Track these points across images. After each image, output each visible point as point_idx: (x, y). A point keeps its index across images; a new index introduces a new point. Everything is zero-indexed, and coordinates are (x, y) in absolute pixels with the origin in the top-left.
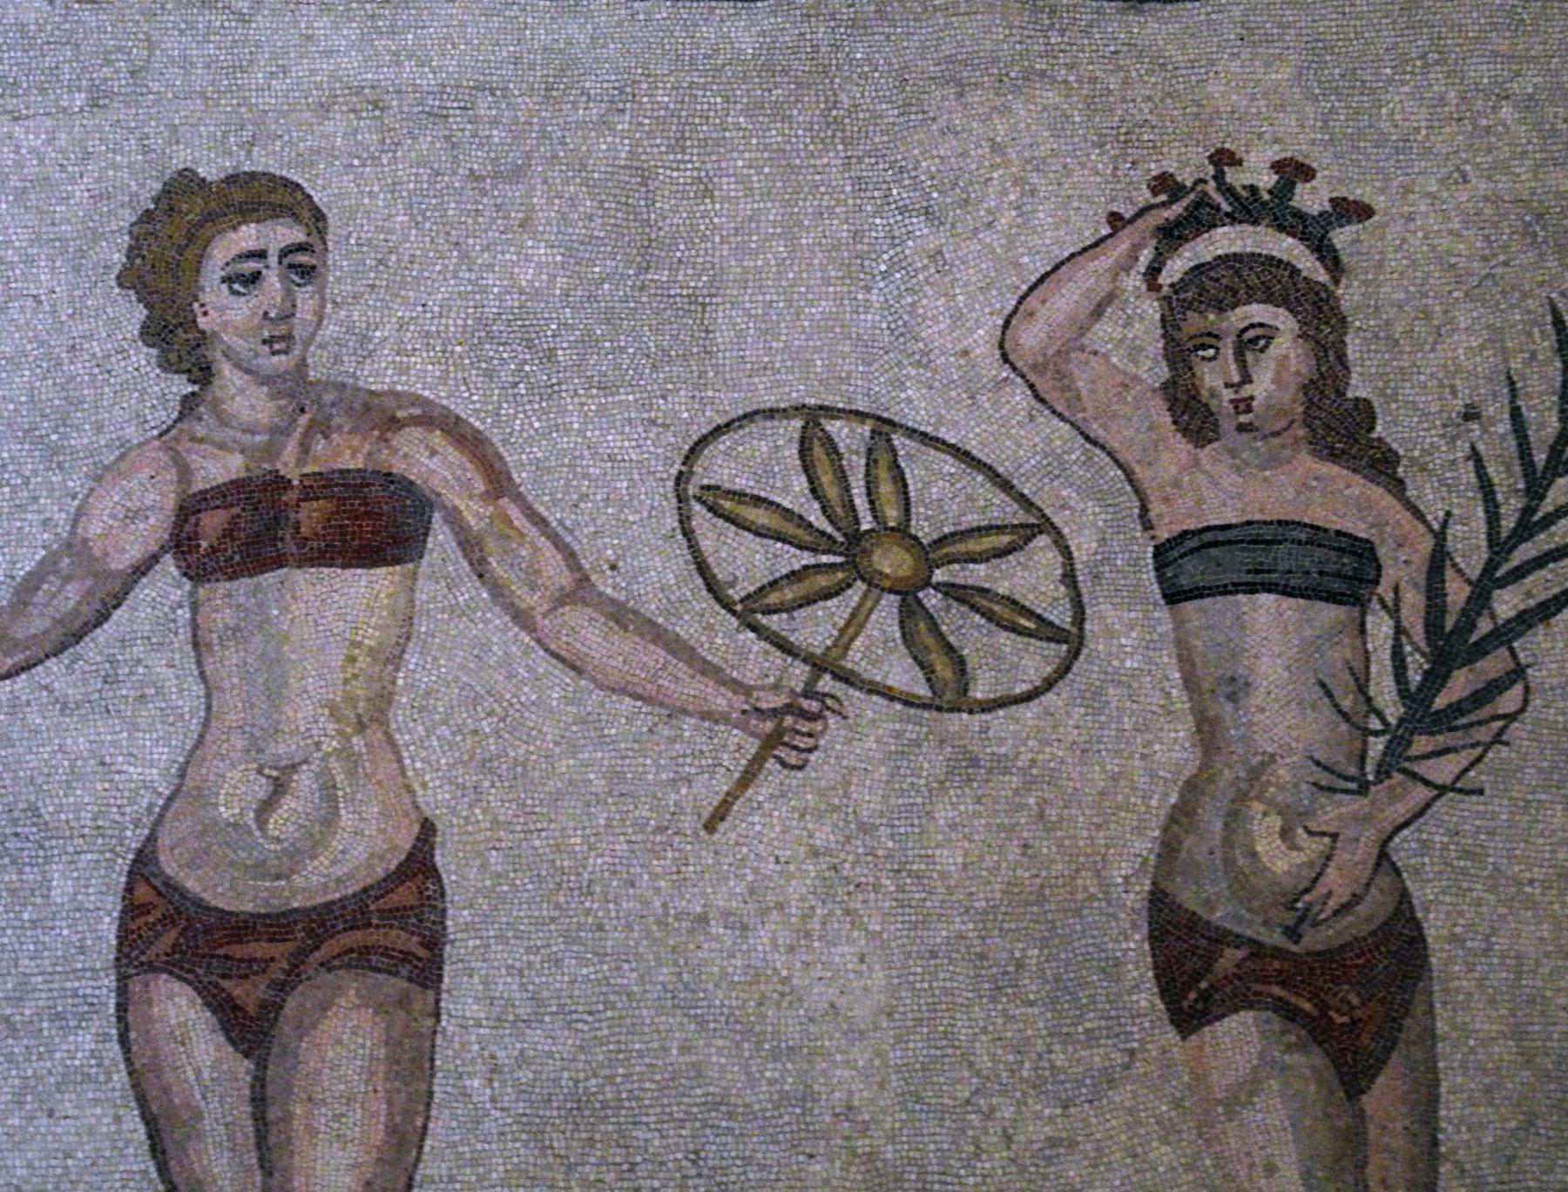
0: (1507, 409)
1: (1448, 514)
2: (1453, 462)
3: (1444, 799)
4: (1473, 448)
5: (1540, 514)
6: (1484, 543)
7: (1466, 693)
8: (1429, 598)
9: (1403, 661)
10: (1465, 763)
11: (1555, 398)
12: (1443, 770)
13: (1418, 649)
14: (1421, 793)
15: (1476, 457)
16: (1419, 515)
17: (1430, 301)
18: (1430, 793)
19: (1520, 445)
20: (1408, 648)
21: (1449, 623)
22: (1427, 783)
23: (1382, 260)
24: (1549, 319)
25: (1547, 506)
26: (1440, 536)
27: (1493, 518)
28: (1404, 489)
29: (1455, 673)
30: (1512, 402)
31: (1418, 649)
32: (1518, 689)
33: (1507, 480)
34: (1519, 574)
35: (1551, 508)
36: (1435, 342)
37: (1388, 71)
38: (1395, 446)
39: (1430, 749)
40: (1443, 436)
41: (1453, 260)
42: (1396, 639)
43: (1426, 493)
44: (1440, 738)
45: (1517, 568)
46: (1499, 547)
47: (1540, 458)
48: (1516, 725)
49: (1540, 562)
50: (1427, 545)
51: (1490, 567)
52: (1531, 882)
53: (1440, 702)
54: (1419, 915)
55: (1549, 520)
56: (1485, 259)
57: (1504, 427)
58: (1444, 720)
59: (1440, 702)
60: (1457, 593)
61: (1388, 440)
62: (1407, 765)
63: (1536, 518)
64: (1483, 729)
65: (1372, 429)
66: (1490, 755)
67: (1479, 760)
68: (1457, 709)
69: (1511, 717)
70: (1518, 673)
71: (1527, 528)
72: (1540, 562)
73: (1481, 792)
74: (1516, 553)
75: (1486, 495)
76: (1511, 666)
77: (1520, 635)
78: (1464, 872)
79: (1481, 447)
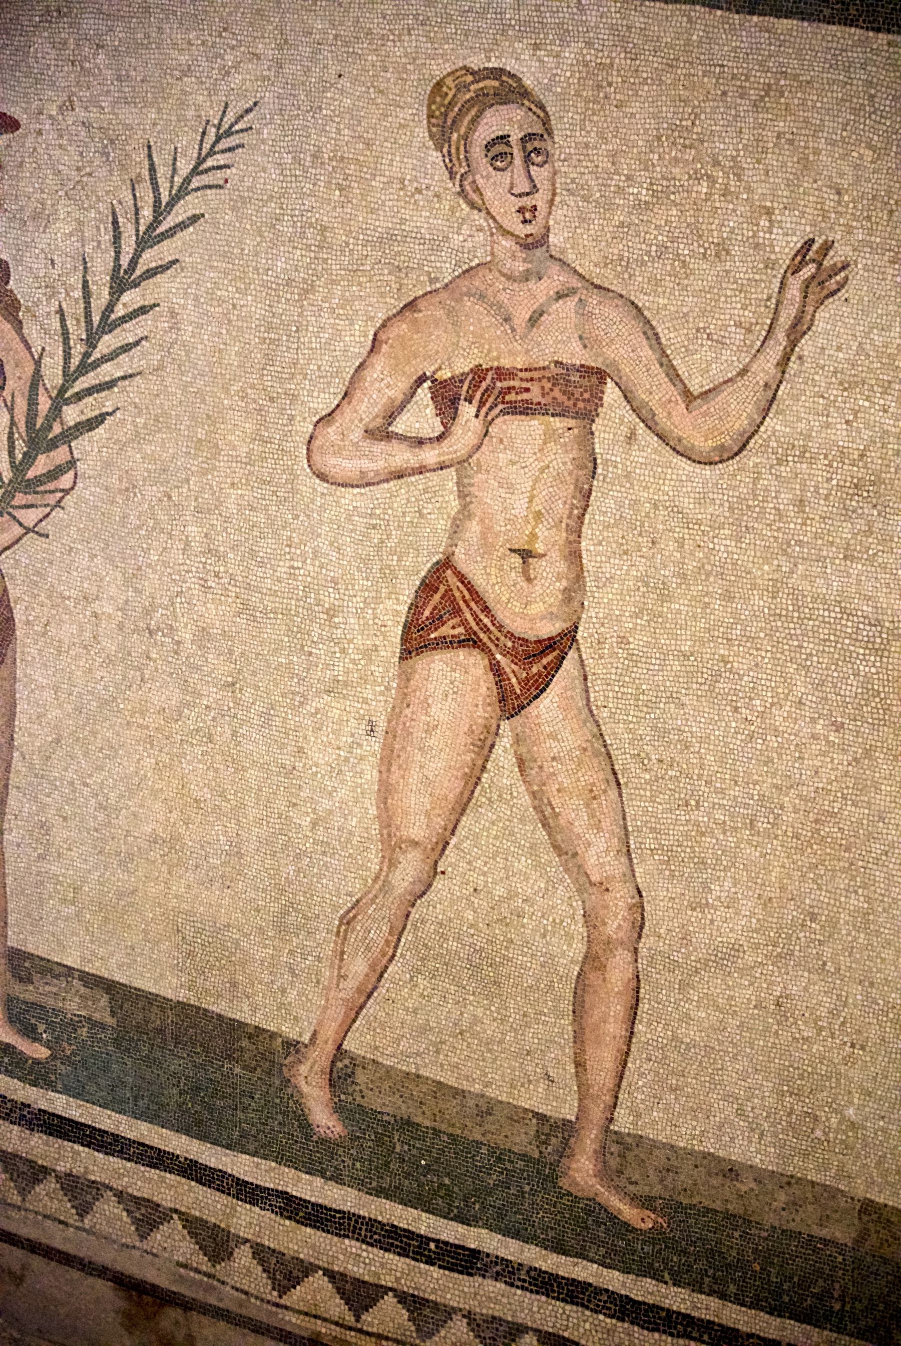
0: (81, 282)
1: (43, 349)
2: (48, 314)
3: (28, 536)
4: (60, 306)
5: (92, 358)
6: (60, 373)
7: (44, 471)
8: (29, 404)
9: (13, 443)
10: (41, 516)
11: (108, 278)
12: (30, 517)
13: (21, 437)
14: (18, 531)
15: (61, 312)
16: (28, 348)
17: (45, 196)
18: (21, 531)
19: (86, 308)
20: (16, 436)
21: (39, 422)
22: (21, 524)
23: (22, 162)
24: (110, 219)
25: (96, 355)
26: (38, 363)
27: (67, 356)
28: (22, 328)
29: (40, 456)
30: (84, 277)
31: (21, 437)
32: (71, 474)
33: (78, 332)
34: (79, 397)
35: (99, 356)
36: (46, 226)
37: (37, 19)
38: (19, 297)
39: (24, 503)
40: (45, 294)
41: (61, 167)
42: (11, 428)
43: (32, 331)
44: (30, 497)
45: (77, 393)
46: (69, 378)
47: (96, 319)
48: (69, 497)
49: (89, 391)
50: (30, 369)
51: (62, 390)
52: (69, 598)
53: (30, 474)
54: (12, 605)
55: (96, 364)
56: (78, 169)
57: (78, 294)
58: (31, 486)
59: (30, 474)
60: (44, 404)
61: (16, 292)
62: (11, 510)
63: (89, 361)
64: (51, 496)
65: (7, 283)
66: (54, 513)
67: (48, 515)
68: (39, 480)
69: (66, 492)
70: (72, 463)
71: (85, 368)
72: (89, 391)
73: (47, 536)
74: (77, 383)
75: (64, 339)
76: (69, 458)
77: (76, 438)
78: (36, 583)
79: (64, 306)
